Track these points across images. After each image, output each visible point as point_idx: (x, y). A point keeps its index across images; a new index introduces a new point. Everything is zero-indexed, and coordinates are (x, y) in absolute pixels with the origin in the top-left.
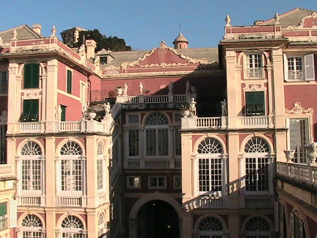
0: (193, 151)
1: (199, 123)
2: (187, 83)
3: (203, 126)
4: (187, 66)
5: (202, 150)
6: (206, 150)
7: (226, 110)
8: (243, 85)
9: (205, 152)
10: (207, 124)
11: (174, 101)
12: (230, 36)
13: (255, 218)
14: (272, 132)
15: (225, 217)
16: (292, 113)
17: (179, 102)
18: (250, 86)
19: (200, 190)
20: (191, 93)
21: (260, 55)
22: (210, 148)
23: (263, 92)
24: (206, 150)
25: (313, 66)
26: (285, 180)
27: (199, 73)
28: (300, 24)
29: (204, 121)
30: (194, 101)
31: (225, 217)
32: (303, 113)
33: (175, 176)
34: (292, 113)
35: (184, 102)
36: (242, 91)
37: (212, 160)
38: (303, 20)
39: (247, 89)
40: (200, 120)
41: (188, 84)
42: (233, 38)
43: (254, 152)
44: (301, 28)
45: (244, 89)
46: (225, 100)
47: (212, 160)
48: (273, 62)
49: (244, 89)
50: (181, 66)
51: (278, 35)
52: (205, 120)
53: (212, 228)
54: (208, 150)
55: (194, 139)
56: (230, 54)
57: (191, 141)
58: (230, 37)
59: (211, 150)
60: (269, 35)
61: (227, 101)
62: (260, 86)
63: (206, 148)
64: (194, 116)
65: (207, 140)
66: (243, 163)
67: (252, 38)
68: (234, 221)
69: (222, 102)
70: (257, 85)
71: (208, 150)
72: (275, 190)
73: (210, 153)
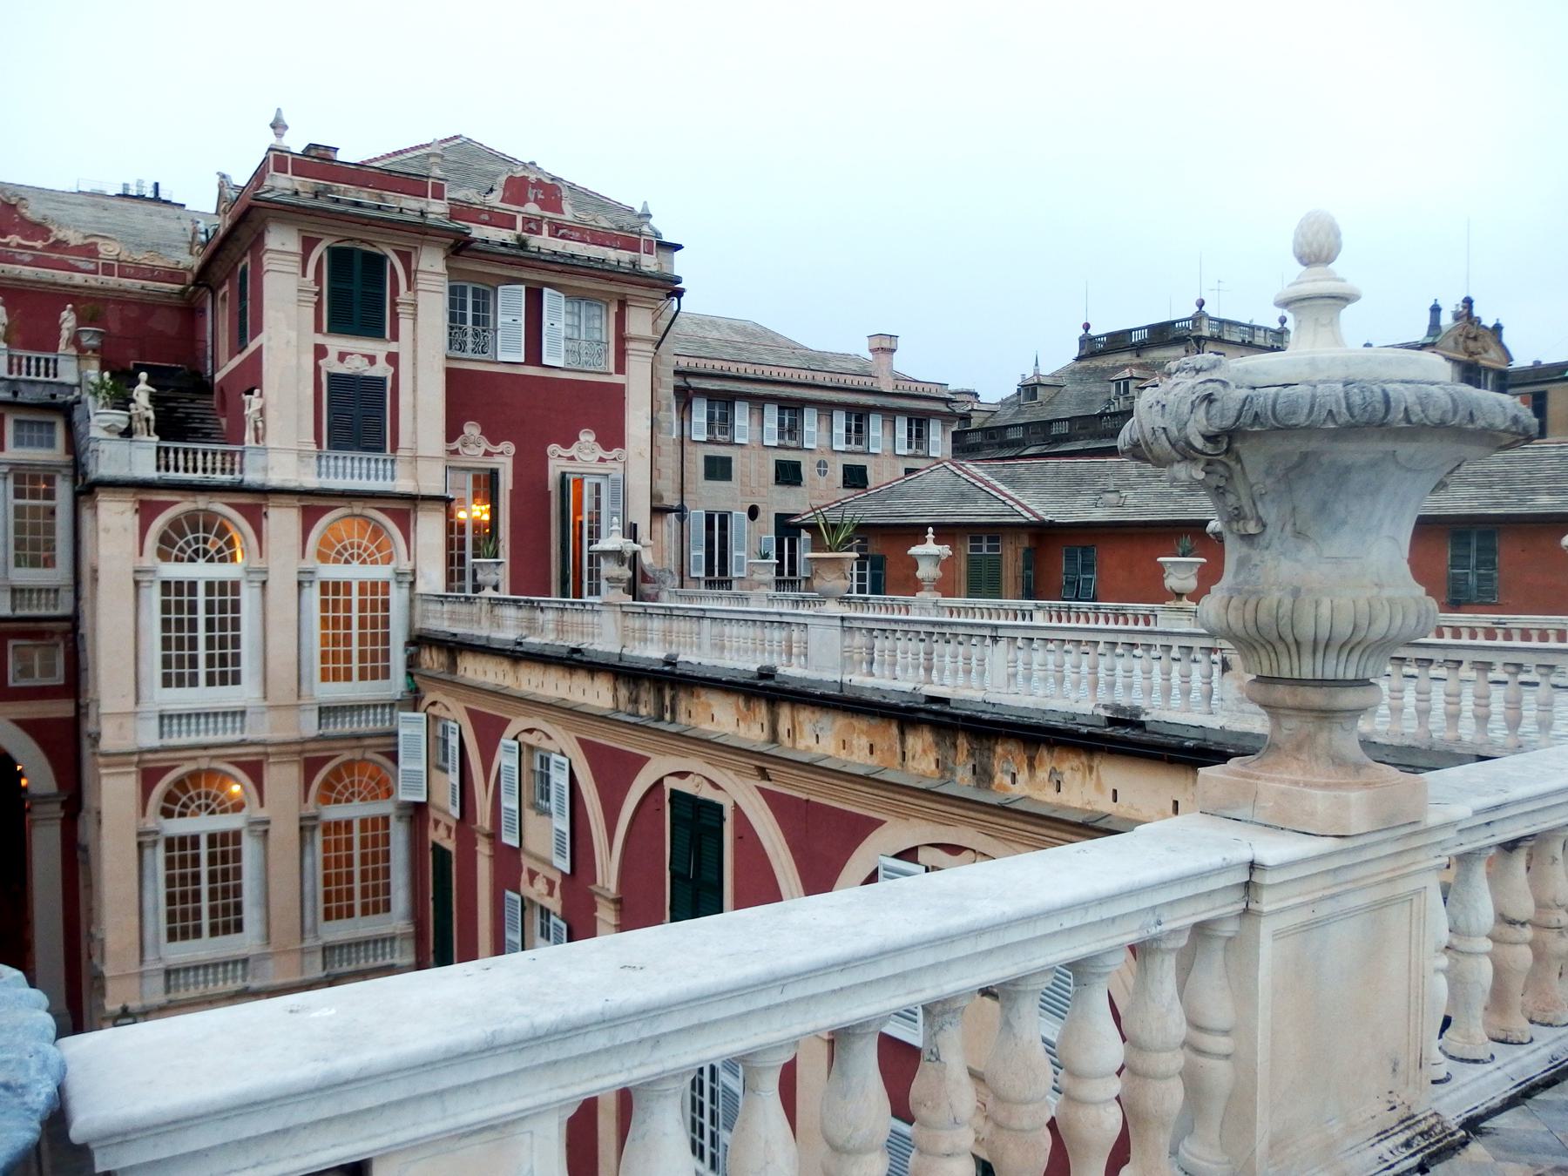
0: (141, 554)
1: (162, 464)
2: (65, 314)
3: (177, 469)
4: (45, 249)
6: (189, 551)
7: (260, 425)
8: (320, 352)
10: (191, 464)
11: (10, 372)
12: (288, 184)
13: (349, 765)
14: (404, 507)
15: (254, 771)
16: (456, 452)
17: (33, 377)
18: (342, 357)
19: (166, 682)
20: (82, 352)
21: (376, 263)
22: (201, 546)
23: (383, 380)
25: (522, 321)
26: (454, 647)
27: (93, 283)
28: (491, 190)
29: (181, 456)
30: (148, 383)
31: (254, 771)
32: (487, 454)
33: (11, 643)
34: (456, 452)
35: (51, 378)
36: (317, 369)
37: (210, 586)
38: (503, 179)
39: (331, 365)
40: (167, 450)
41: (68, 320)
42: (296, 193)
43: (347, 562)
44: (494, 200)
45: (321, 362)
46: (257, 392)
47: (210, 586)
48: (416, 291)
49: (321, 362)
50: (19, 246)
51: (437, 209)
52: (186, 452)
53: (207, 806)
54: (196, 551)
55: (147, 513)
56: (281, 242)
57: (137, 517)
58: (283, 184)
60: (411, 203)
61: (261, 396)
63: (190, 546)
64: (145, 437)
65: (192, 518)
66: (313, 596)
67: (357, 204)
68: (283, 779)
69: (247, 398)
71: (196, 551)
72: (410, 675)
73: (201, 561)
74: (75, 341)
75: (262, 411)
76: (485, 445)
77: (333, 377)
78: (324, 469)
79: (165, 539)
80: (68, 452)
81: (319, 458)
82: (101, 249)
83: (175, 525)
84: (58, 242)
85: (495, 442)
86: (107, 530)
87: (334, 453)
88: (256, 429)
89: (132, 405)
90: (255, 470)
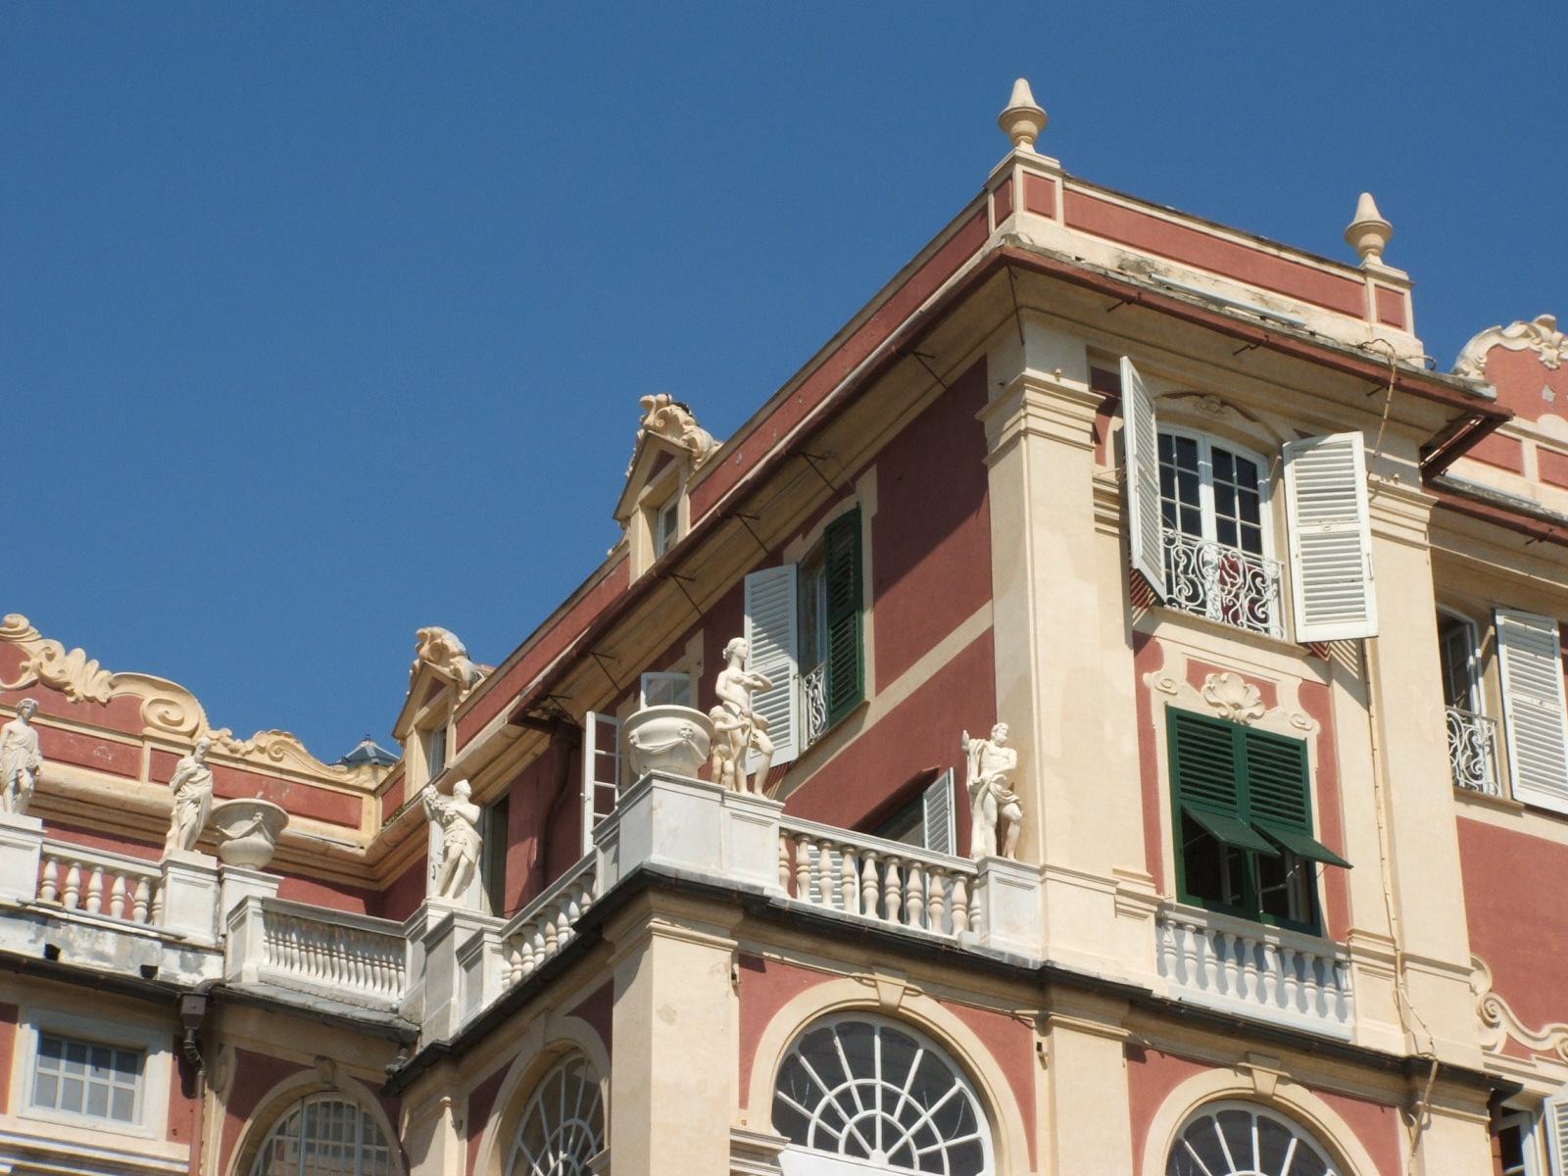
5: (815, 1118)
6: (850, 1124)
7: (1012, 810)
9: (842, 1137)
18: (1197, 673)
22: (878, 1112)
24: (850, 1124)
32: (1513, 1048)
36: (1143, 695)
59: (891, 1135)
62: (1268, 694)
63: (851, 1110)
69: (973, 744)
70: (1248, 680)
71: (866, 1127)
73: (879, 1156)
74: (208, 838)
75: (1012, 782)
76: (1508, 1025)
77: (1182, 723)
78: (1170, 958)
79: (789, 1075)
80: (175, 1133)
81: (1161, 922)
82: (153, 714)
83: (813, 1041)
84: (44, 681)
85: (1531, 1019)
86: (669, 1015)
87: (1197, 916)
88: (1002, 826)
89: (717, 710)
90: (1013, 927)
